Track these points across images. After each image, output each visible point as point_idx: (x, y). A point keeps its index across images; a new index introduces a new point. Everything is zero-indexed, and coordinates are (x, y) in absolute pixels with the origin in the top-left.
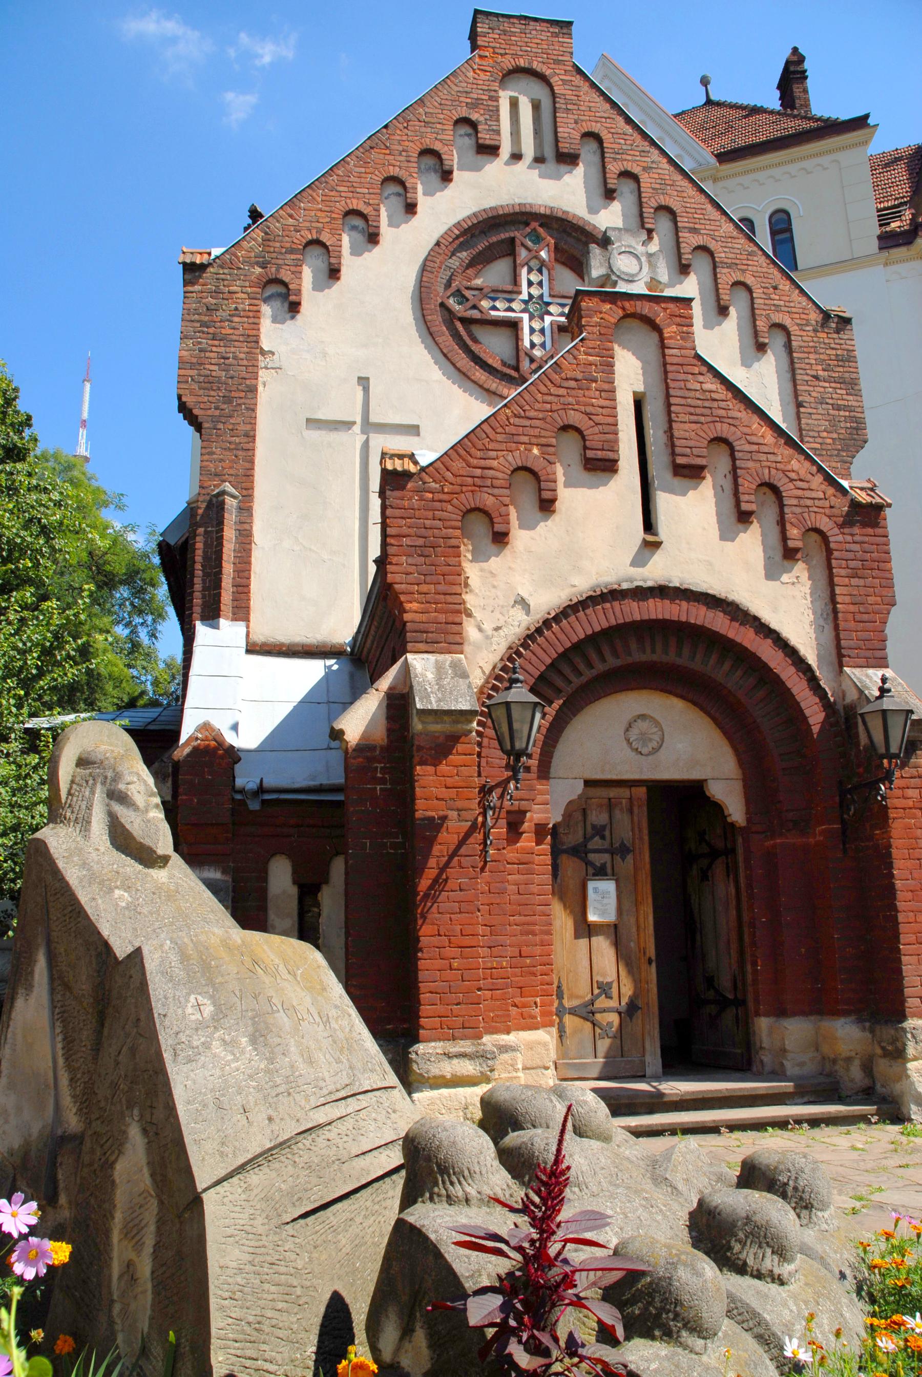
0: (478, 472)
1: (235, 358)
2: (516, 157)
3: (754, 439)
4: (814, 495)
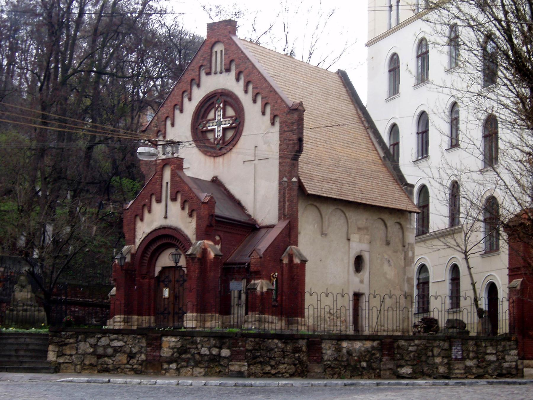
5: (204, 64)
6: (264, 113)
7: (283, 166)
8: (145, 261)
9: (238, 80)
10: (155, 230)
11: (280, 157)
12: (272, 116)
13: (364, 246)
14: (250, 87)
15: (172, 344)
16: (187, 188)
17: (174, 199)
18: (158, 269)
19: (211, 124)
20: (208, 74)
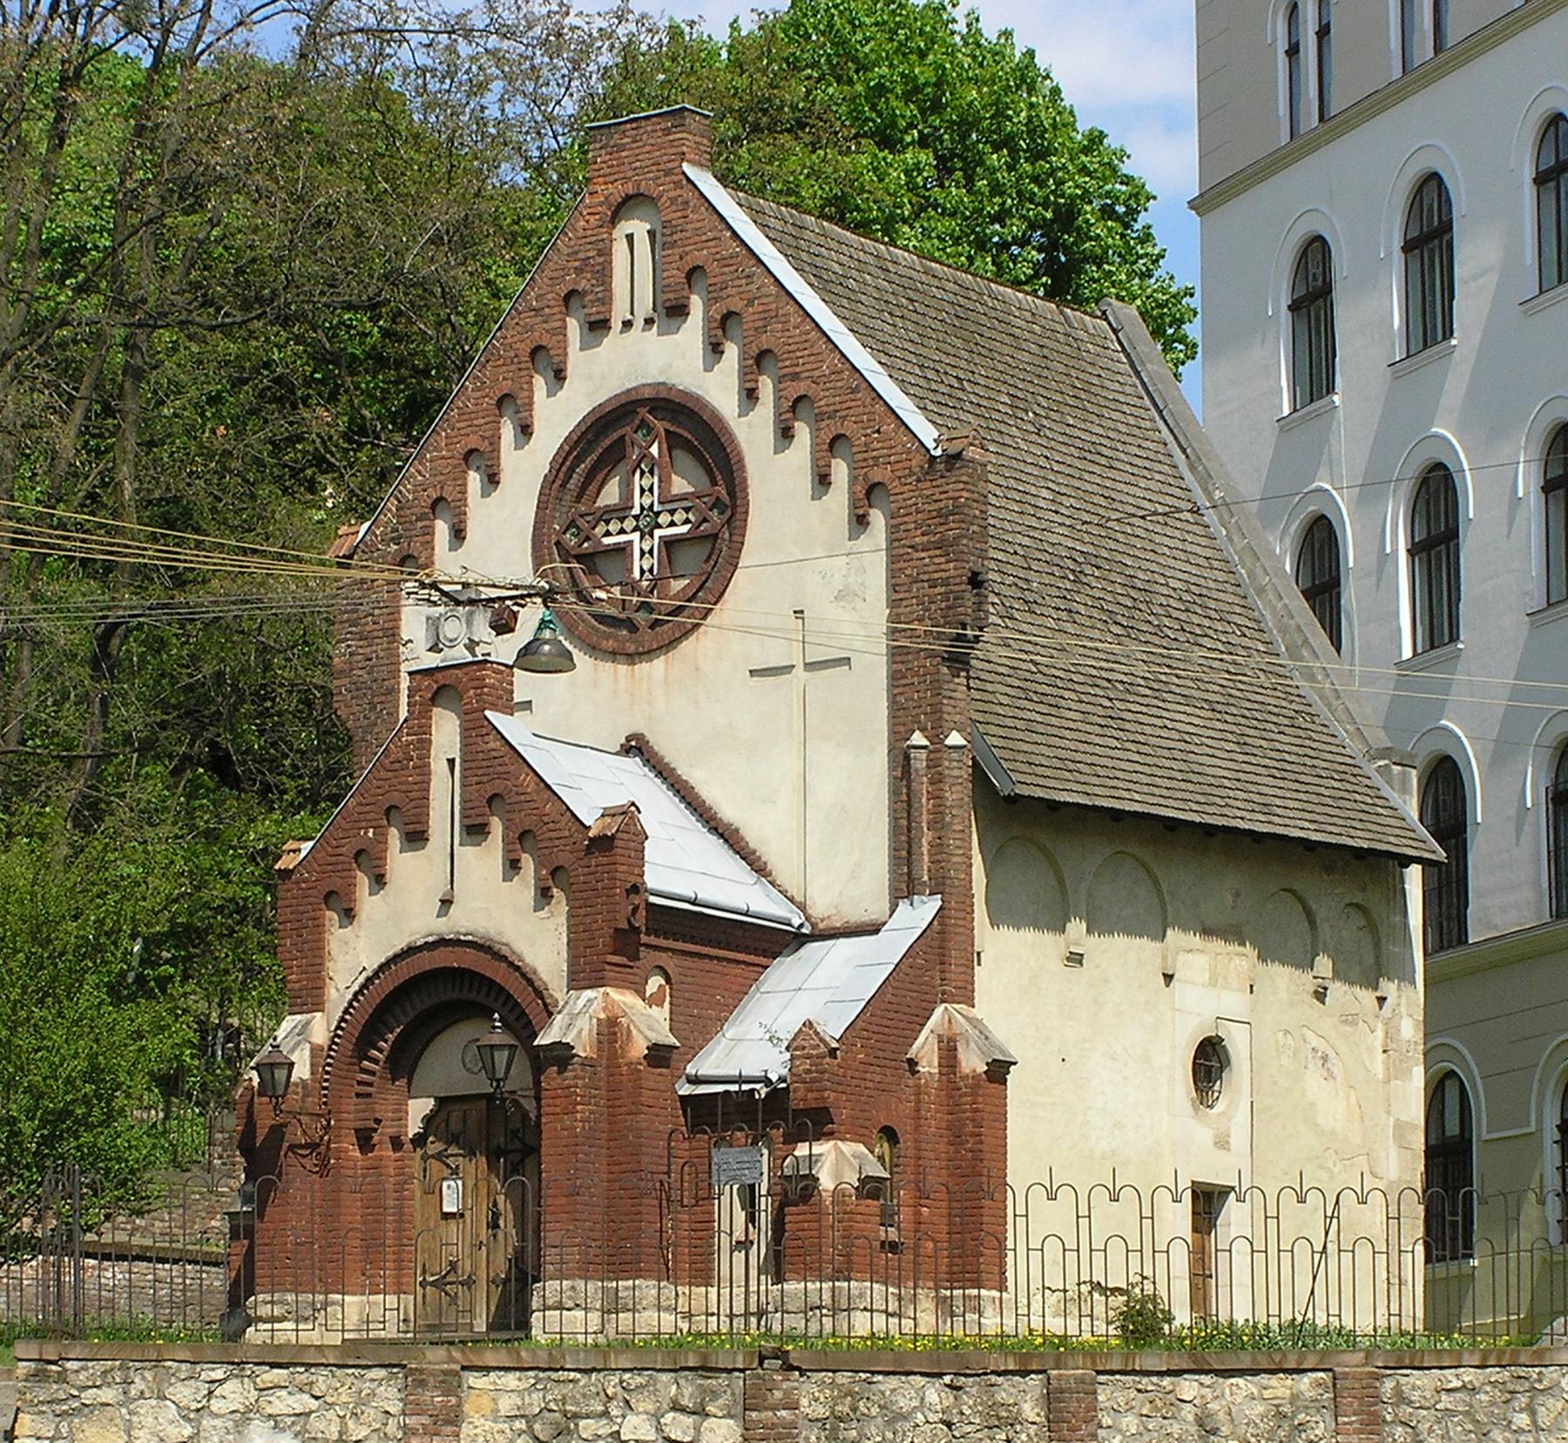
2: (627, 325)
3: (521, 790)
5: (583, 285)
6: (823, 480)
9: (715, 349)
10: (410, 951)
12: (860, 491)
13: (1233, 1002)
15: (506, 1404)
19: (614, 526)
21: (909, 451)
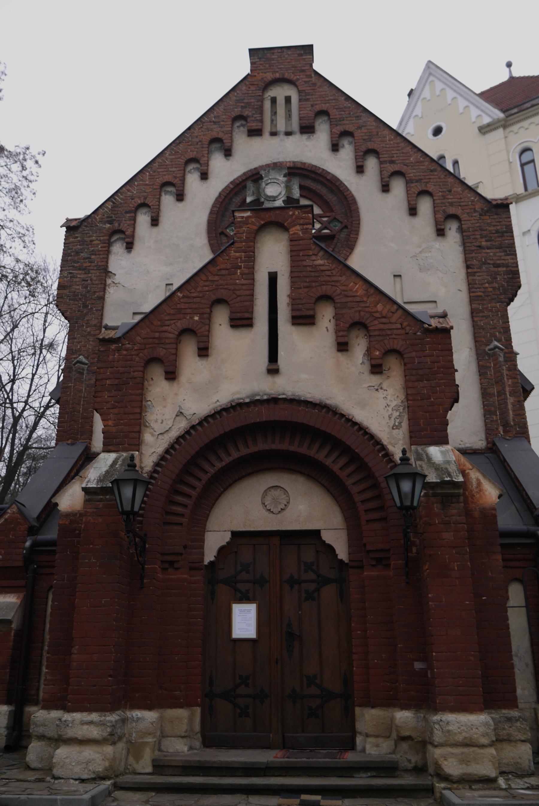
0: (157, 335)
1: (91, 280)
3: (350, 294)
4: (393, 326)
7: (487, 317)
8: (179, 509)
9: (335, 148)
11: (472, 300)
12: (440, 216)
14: (372, 163)
16: (359, 289)
17: (303, 319)
18: (214, 541)
20: (255, 133)
21: (473, 201)
